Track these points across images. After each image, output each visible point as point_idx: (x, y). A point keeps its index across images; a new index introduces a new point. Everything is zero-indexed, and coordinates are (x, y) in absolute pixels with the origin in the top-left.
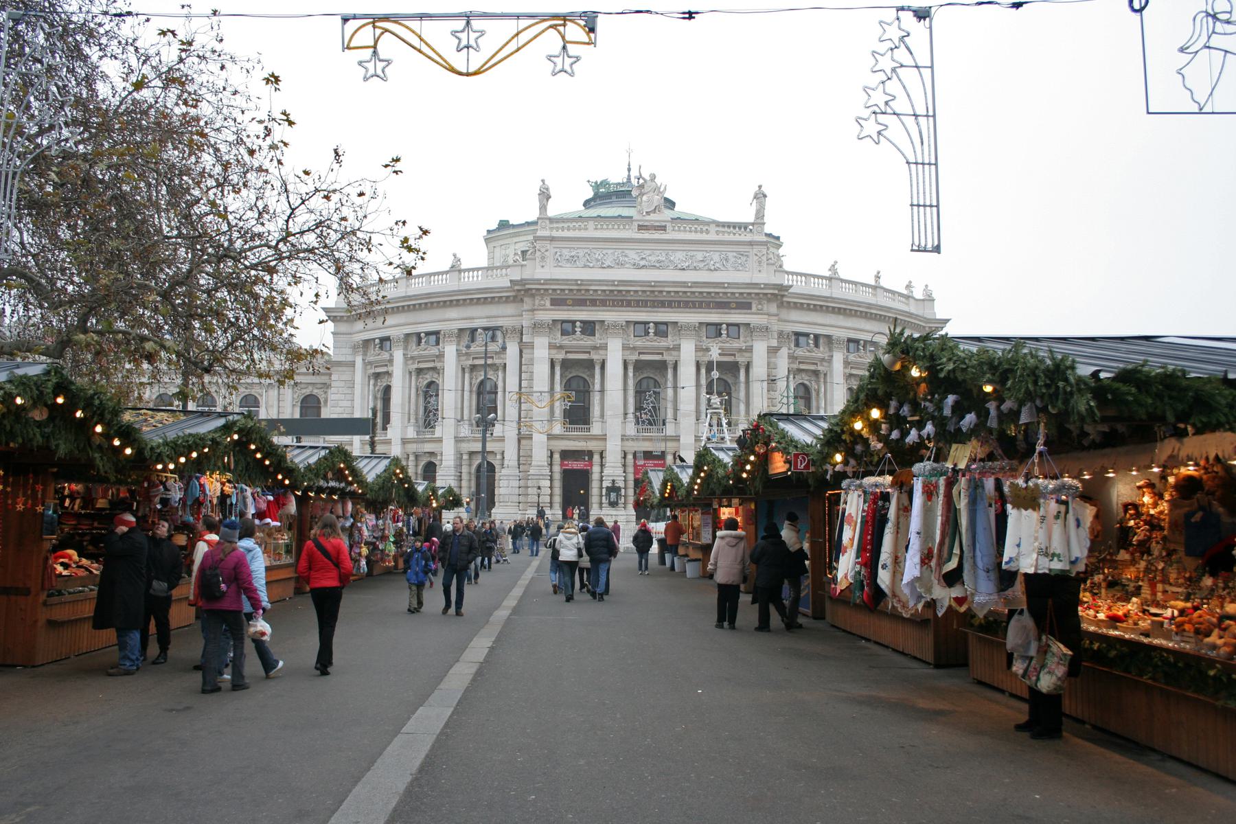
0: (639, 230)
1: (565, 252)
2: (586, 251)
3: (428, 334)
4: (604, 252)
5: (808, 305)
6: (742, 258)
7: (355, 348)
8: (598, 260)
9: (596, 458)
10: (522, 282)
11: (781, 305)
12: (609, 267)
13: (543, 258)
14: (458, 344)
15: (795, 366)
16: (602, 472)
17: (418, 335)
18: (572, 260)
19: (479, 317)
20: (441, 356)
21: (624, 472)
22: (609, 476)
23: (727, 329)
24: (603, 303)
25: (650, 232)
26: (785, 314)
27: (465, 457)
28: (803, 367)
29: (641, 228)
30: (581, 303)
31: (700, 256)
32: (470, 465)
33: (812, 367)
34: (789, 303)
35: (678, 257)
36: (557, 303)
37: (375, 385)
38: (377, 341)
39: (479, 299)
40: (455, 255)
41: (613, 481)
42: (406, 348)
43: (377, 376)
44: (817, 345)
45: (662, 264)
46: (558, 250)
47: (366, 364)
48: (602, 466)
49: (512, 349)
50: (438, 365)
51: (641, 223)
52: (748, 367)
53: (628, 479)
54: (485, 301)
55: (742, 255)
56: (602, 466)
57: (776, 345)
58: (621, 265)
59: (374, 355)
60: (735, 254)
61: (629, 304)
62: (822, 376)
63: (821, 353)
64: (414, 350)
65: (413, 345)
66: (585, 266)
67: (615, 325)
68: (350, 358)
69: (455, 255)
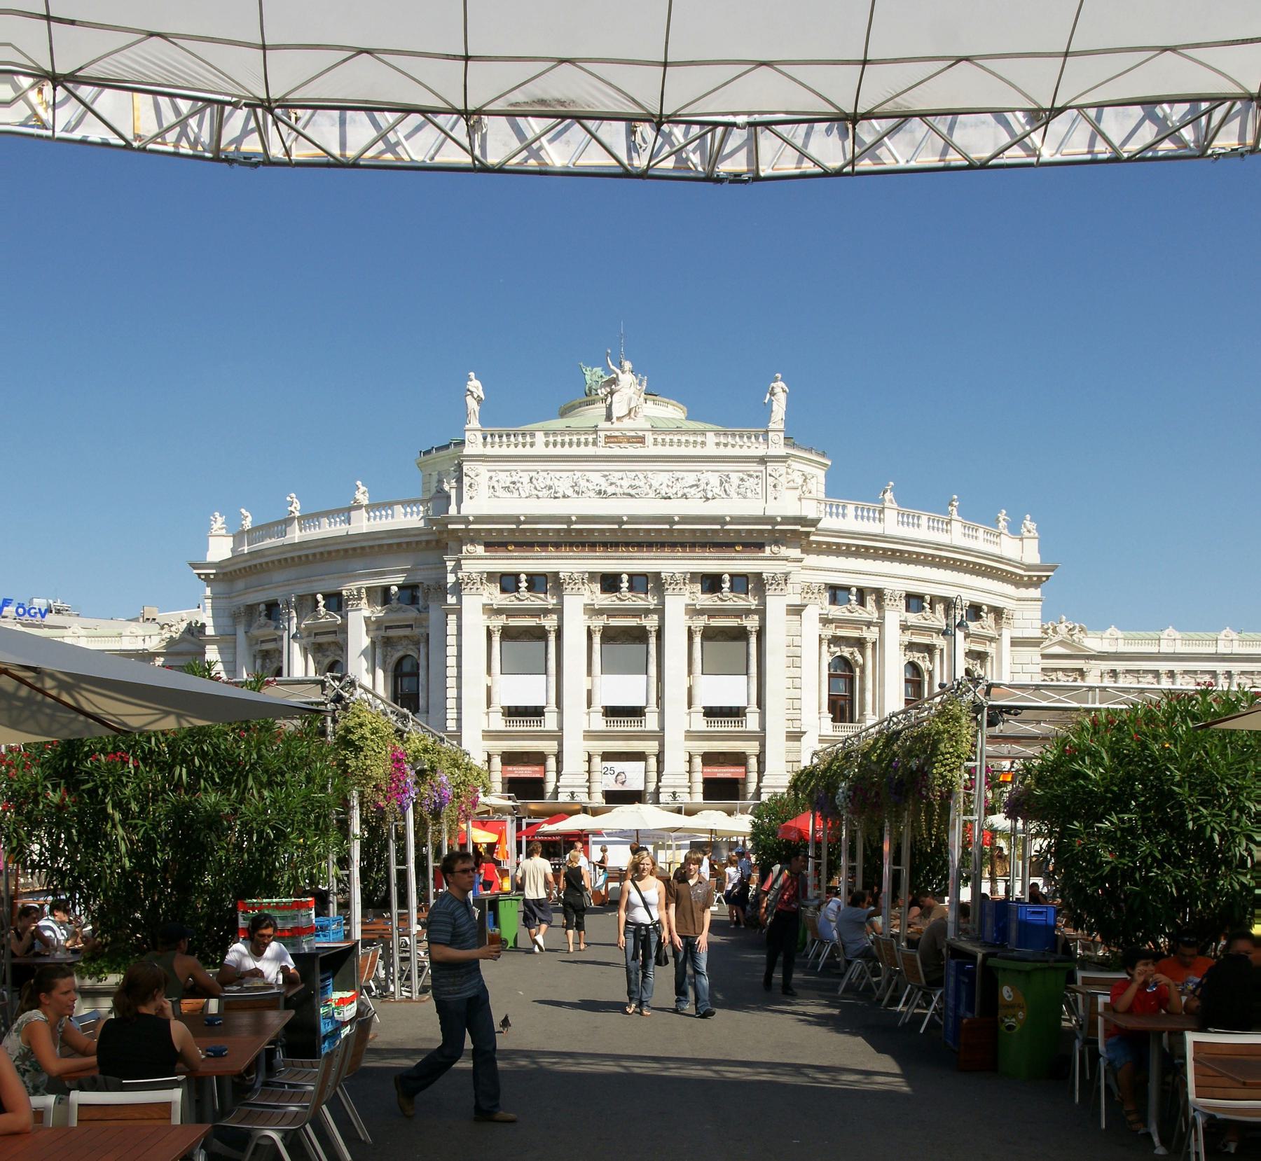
0: (606, 443)
1: (502, 476)
2: (534, 474)
4: (558, 474)
5: (848, 546)
6: (751, 479)
9: (551, 763)
11: (809, 548)
16: (558, 780)
21: (589, 781)
22: (566, 786)
23: (731, 581)
25: (622, 445)
28: (841, 633)
29: (610, 439)
31: (691, 478)
33: (854, 634)
34: (818, 543)
35: (661, 479)
38: (262, 607)
39: (390, 545)
41: (572, 793)
43: (266, 655)
44: (862, 602)
45: (638, 490)
46: (493, 474)
47: (252, 641)
48: (559, 772)
51: (608, 433)
52: (761, 633)
53: (593, 790)
55: (750, 476)
56: (559, 772)
57: (799, 603)
59: (262, 630)
60: (741, 475)
62: (869, 646)
63: (870, 611)
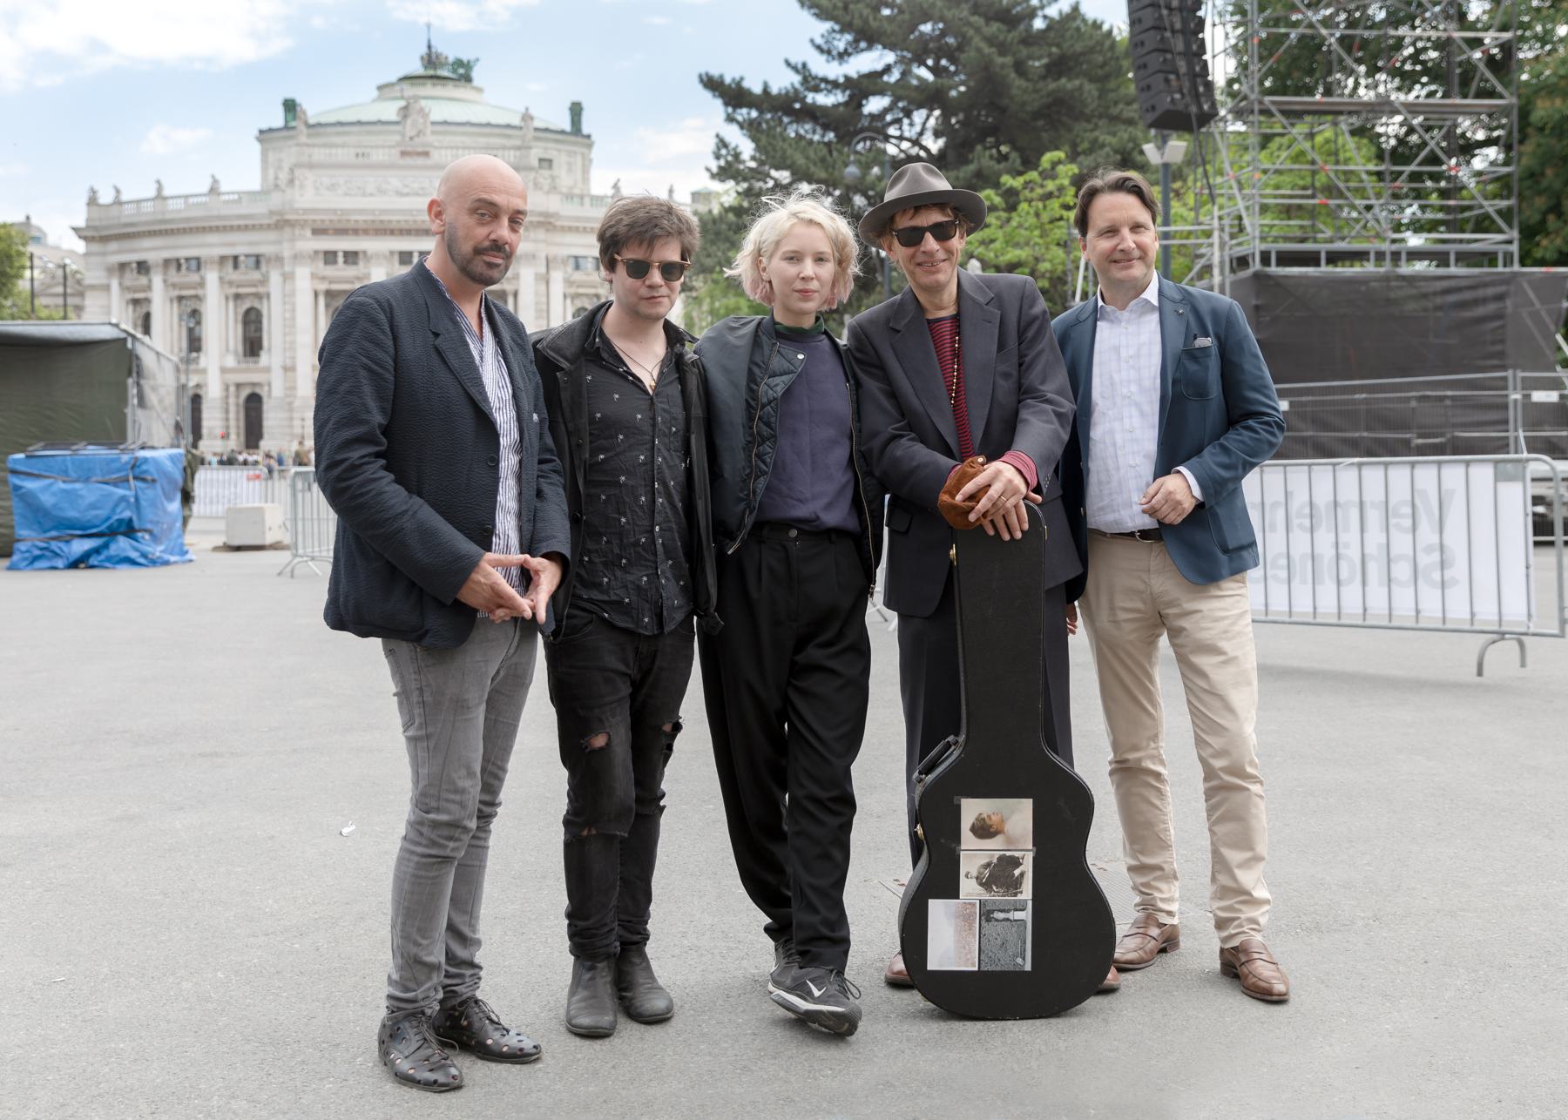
3: (187, 259)
7: (110, 270)
8: (359, 188)
10: (280, 213)
12: (371, 195)
13: (302, 186)
14: (220, 271)
15: (572, 290)
17: (178, 260)
18: (332, 187)
19: (241, 245)
20: (202, 284)
24: (366, 232)
26: (558, 238)
27: (232, 389)
28: (582, 291)
30: (342, 232)
32: (237, 396)
33: (592, 291)
36: (318, 232)
37: (134, 311)
38: (134, 265)
40: (213, 177)
42: (165, 273)
43: (136, 302)
49: (275, 278)
50: (200, 292)
52: (516, 295)
54: (246, 228)
58: (382, 192)
61: (392, 232)
64: (174, 277)
65: (172, 270)
66: (346, 194)
67: (377, 255)
68: (104, 281)
69: (213, 177)
